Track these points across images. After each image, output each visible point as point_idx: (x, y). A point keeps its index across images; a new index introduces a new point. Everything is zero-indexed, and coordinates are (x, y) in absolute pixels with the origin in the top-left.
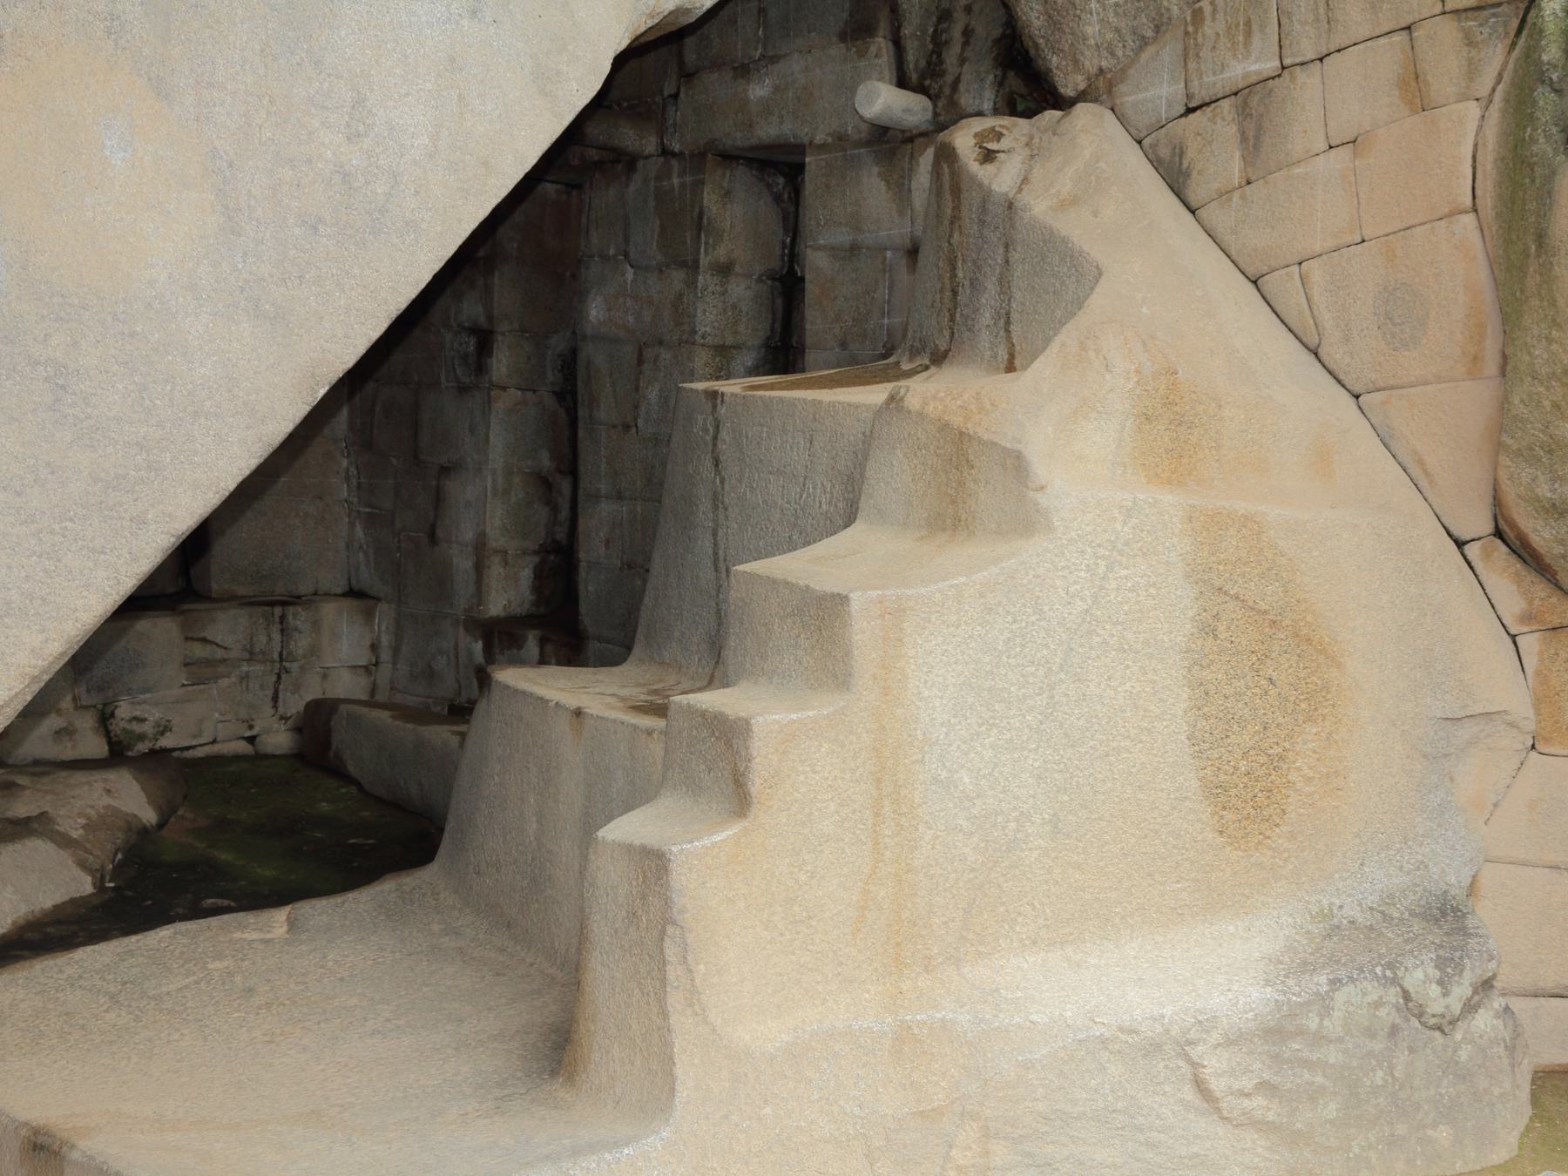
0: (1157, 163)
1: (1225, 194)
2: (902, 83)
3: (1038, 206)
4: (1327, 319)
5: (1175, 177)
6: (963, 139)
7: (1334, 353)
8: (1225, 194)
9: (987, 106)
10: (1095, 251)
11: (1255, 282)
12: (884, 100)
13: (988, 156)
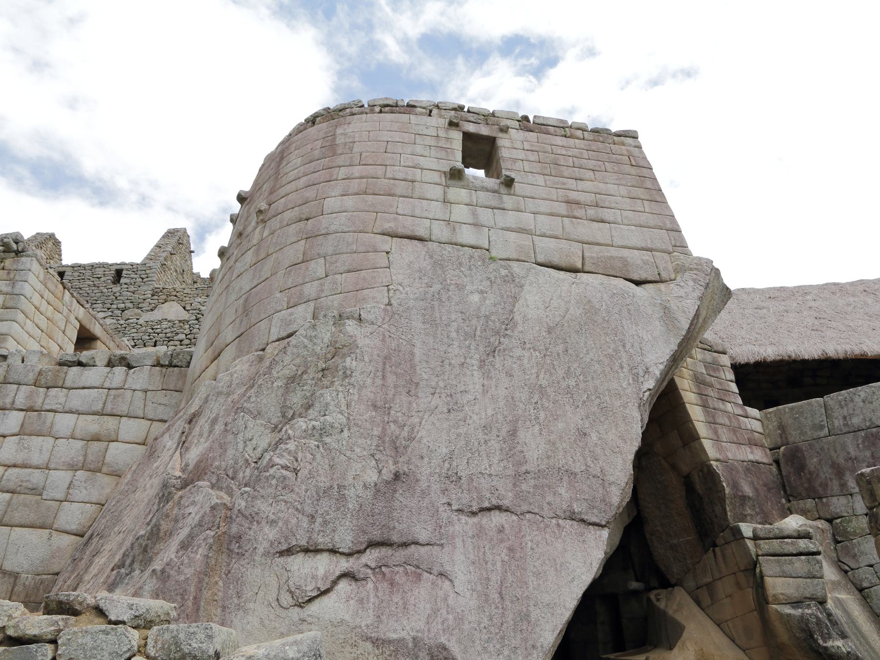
0: (694, 600)
1: (708, 606)
2: (637, 580)
3: (670, 612)
4: (734, 634)
5: (698, 603)
6: (652, 596)
7: (738, 642)
8: (708, 606)
9: (656, 585)
10: (683, 622)
11: (719, 626)
12: (634, 585)
13: (658, 600)
